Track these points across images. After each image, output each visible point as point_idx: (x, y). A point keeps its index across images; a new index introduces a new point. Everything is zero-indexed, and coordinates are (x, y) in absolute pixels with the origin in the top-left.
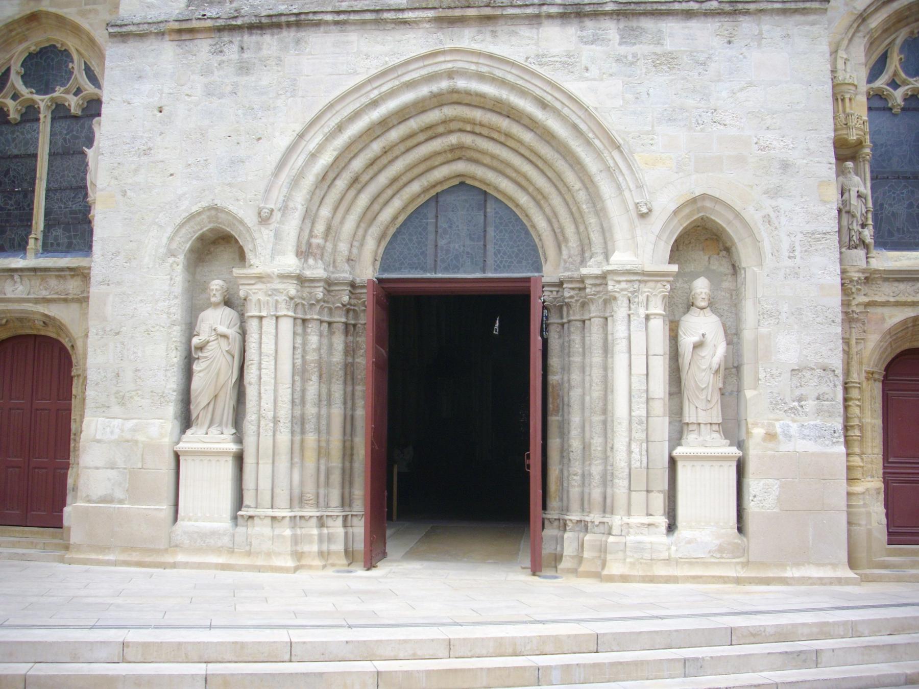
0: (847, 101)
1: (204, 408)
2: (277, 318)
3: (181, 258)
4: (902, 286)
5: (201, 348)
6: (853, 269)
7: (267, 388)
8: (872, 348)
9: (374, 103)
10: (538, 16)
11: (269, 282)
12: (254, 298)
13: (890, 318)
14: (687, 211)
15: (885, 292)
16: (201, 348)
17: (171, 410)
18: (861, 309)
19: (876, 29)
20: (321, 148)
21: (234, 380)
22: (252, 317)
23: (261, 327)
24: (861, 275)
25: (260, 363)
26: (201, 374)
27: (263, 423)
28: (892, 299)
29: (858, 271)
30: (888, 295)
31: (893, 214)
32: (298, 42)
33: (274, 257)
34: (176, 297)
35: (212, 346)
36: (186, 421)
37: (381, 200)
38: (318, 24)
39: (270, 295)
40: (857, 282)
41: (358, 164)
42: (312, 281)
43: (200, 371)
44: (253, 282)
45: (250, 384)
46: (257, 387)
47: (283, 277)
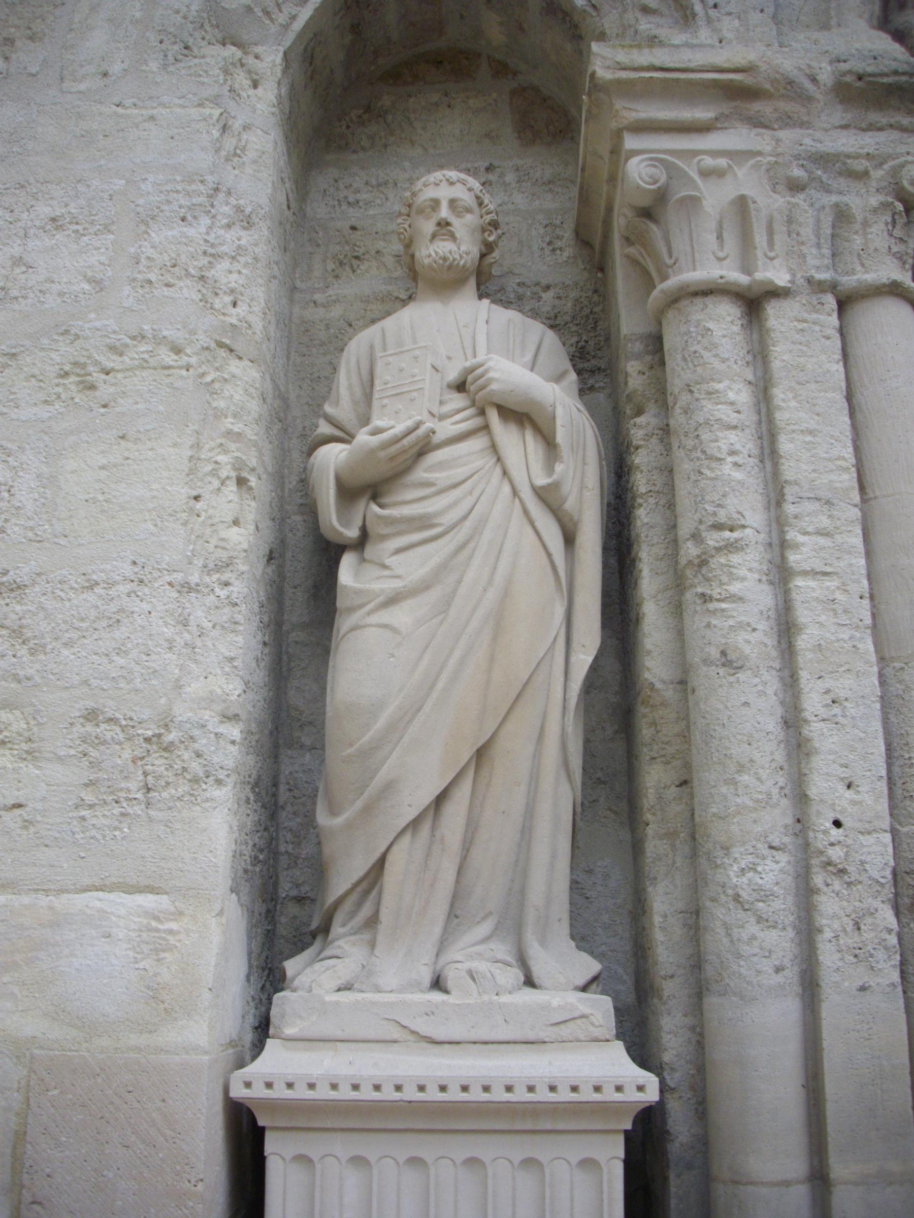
1: (415, 824)
2: (844, 304)
3: (270, 59)
5: (367, 487)
7: (843, 685)
11: (788, 121)
12: (715, 198)
16: (367, 487)
17: (214, 831)
21: (583, 660)
22: (707, 291)
23: (760, 355)
25: (780, 546)
26: (401, 616)
27: (831, 907)
34: (248, 223)
35: (459, 462)
36: (290, 907)
39: (795, 187)
43: (393, 600)
44: (702, 114)
45: (729, 661)
46: (772, 684)
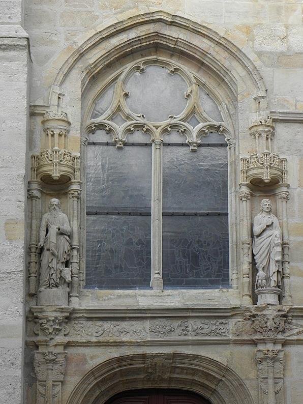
0: (56, 136)
4: (107, 325)
6: (50, 308)
13: (92, 358)
15: (87, 331)
18: (60, 349)
19: (95, 64)
28: (94, 340)
29: (55, 311)
30: (91, 336)
31: (112, 251)
40: (54, 321)
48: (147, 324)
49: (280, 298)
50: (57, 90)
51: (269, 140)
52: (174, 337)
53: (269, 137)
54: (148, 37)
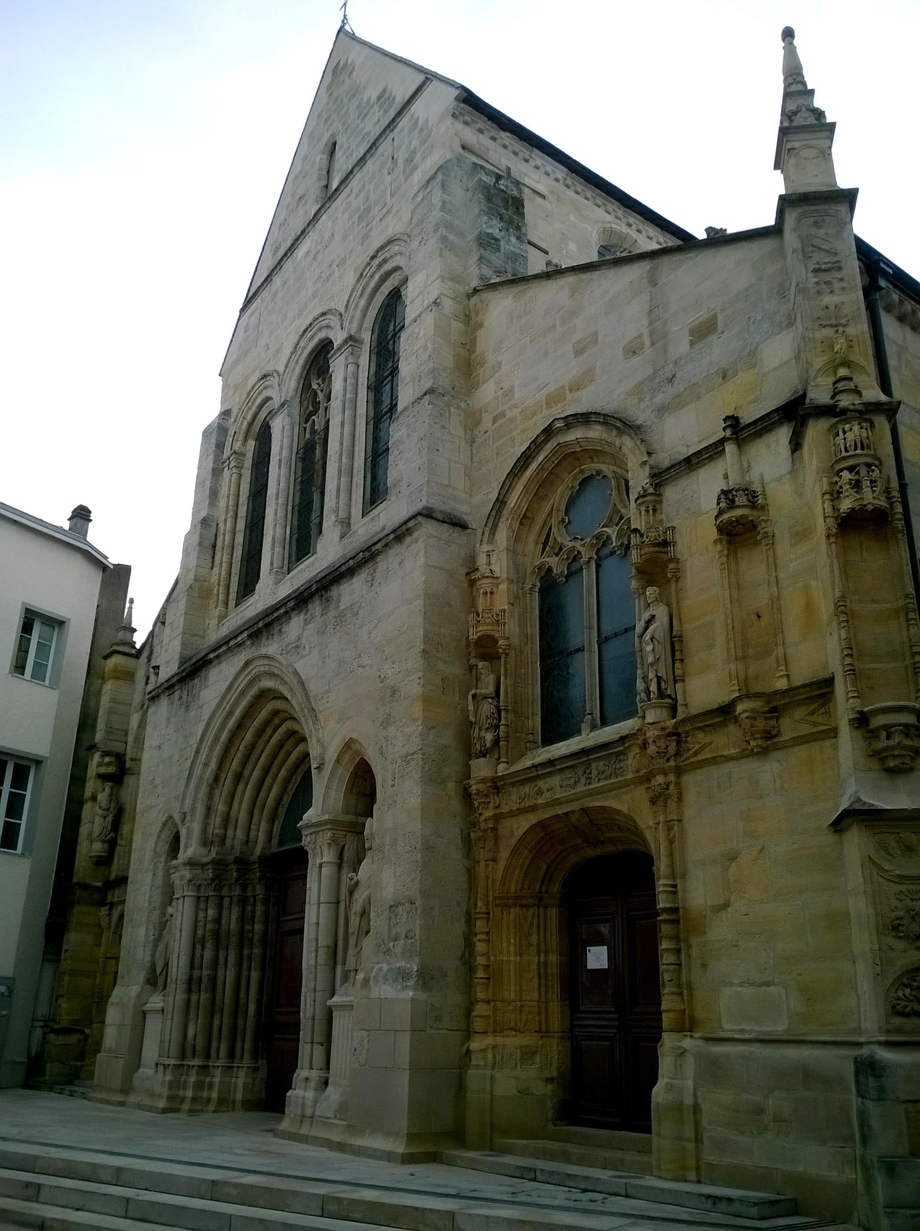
8: (501, 867)
9: (230, 714)
10: (286, 612)
14: (346, 757)
15: (512, 800)
20: (209, 757)
24: (481, 786)
32: (206, 678)
33: (190, 849)
37: (265, 788)
38: (210, 662)
41: (235, 765)
42: (206, 864)
47: (184, 864)
48: (555, 781)
49: (673, 710)
50: (485, 548)
51: (651, 512)
52: (581, 788)
53: (651, 507)
54: (554, 452)
